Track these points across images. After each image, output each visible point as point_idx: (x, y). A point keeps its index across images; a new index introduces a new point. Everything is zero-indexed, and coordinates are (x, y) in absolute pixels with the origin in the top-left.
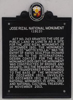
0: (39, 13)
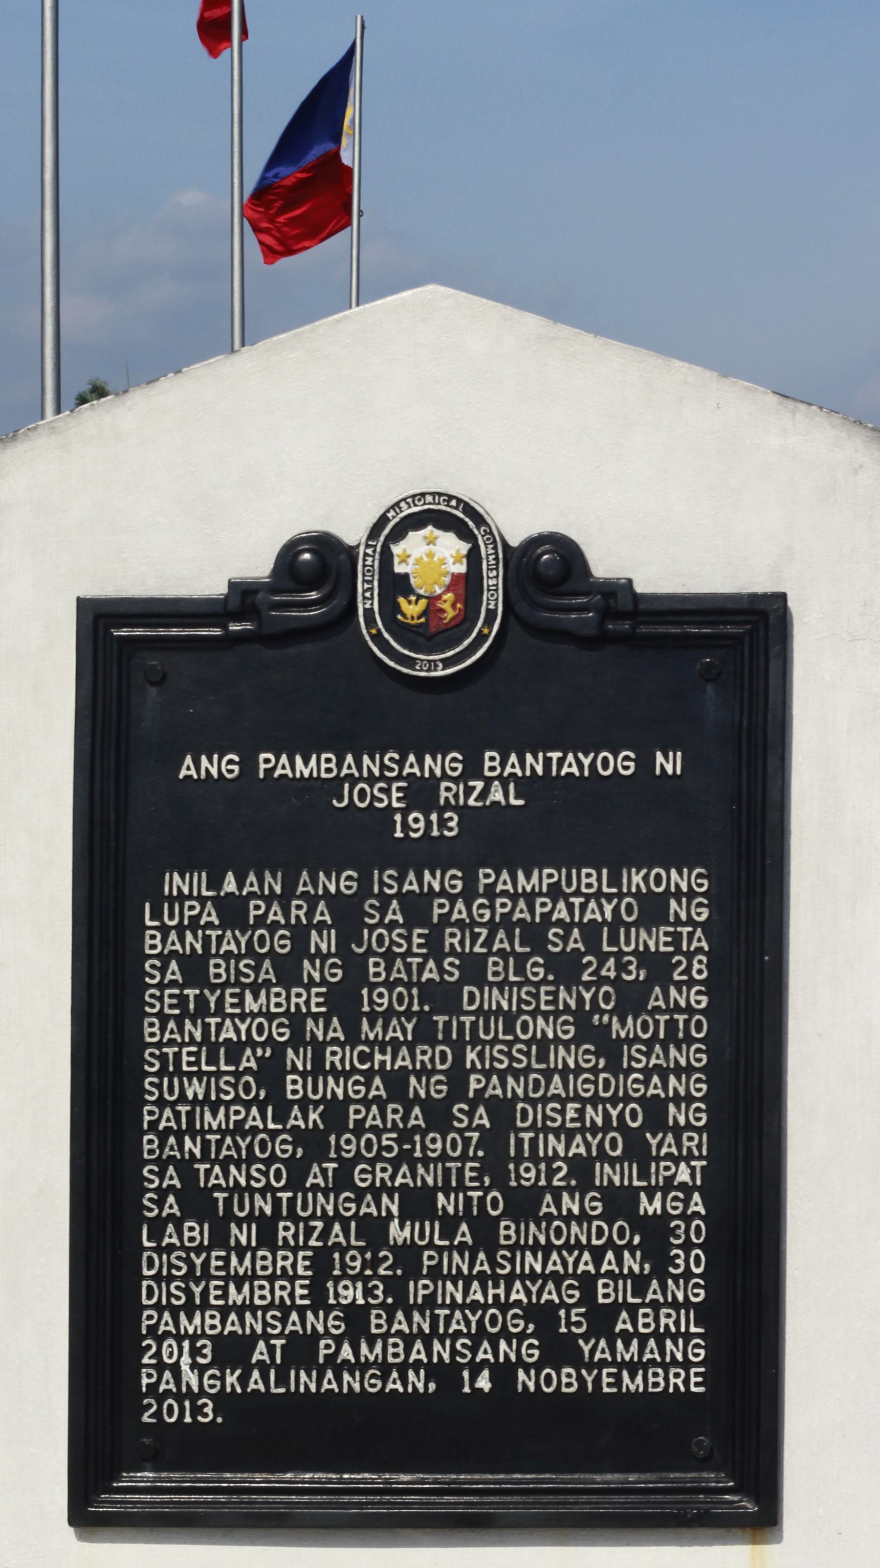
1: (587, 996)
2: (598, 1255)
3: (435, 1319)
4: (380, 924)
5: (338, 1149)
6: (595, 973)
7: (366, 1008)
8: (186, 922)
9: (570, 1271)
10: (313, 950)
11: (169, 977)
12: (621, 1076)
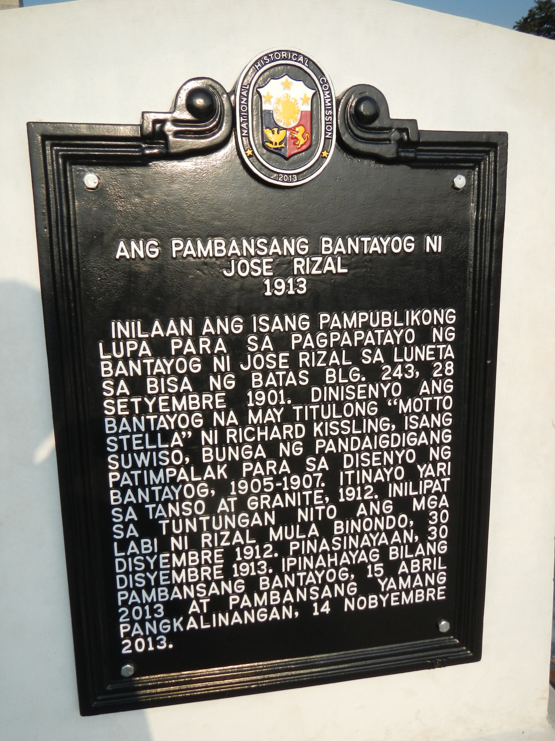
0: (301, 129)
1: (385, 389)
2: (389, 534)
3: (297, 579)
5: (237, 489)
6: (390, 375)
7: (251, 404)
8: (129, 355)
9: (374, 544)
10: (215, 370)
11: (119, 391)
12: (404, 434)
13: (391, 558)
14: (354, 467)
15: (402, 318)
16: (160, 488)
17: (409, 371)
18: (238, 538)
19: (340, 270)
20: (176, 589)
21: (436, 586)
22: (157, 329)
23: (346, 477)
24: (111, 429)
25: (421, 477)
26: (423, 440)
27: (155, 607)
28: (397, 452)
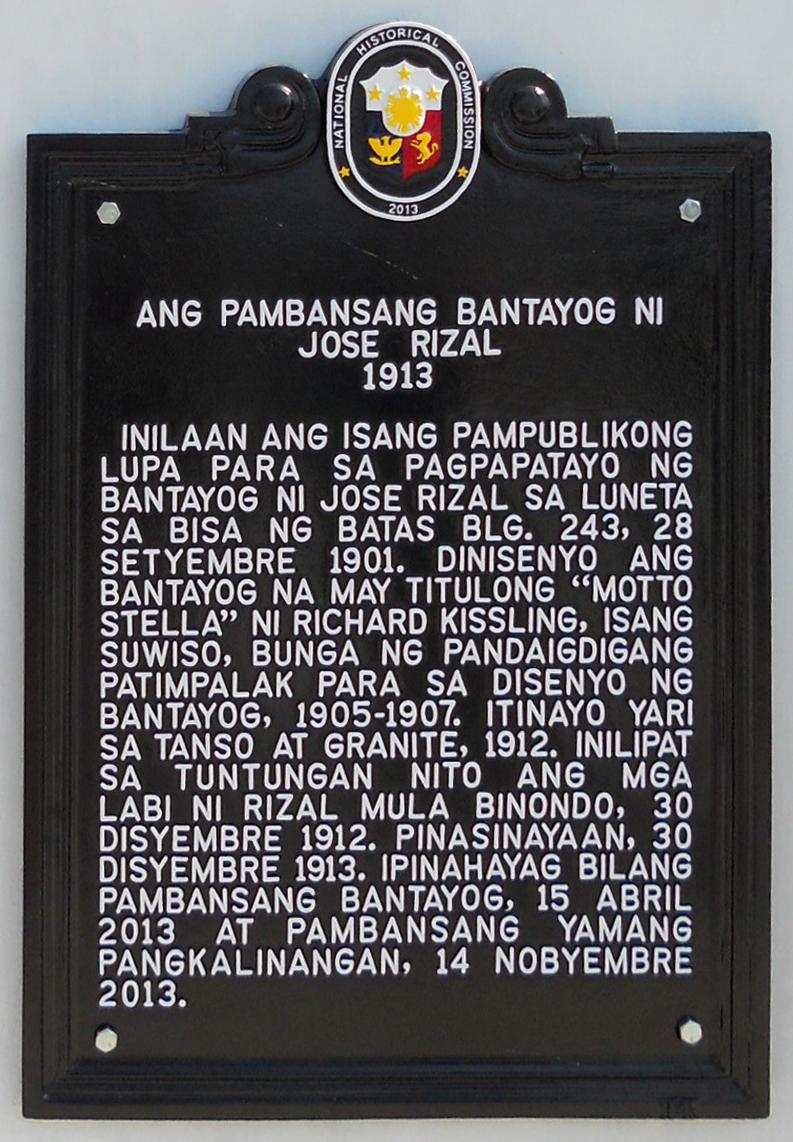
0: (427, 137)
1: (568, 556)
2: (580, 829)
3: (409, 896)
4: (351, 481)
6: (576, 531)
7: (336, 570)
8: (145, 478)
9: (551, 846)
10: (280, 509)
11: (127, 536)
12: (603, 641)
13: (583, 877)
14: (511, 695)
15: (595, 434)
16: (181, 705)
17: (611, 527)
18: (306, 809)
19: (489, 352)
20: (197, 893)
21: (673, 945)
22: (191, 439)
23: (498, 710)
24: (110, 598)
25: (637, 723)
26: (638, 653)
27: (160, 924)
28: (590, 672)
